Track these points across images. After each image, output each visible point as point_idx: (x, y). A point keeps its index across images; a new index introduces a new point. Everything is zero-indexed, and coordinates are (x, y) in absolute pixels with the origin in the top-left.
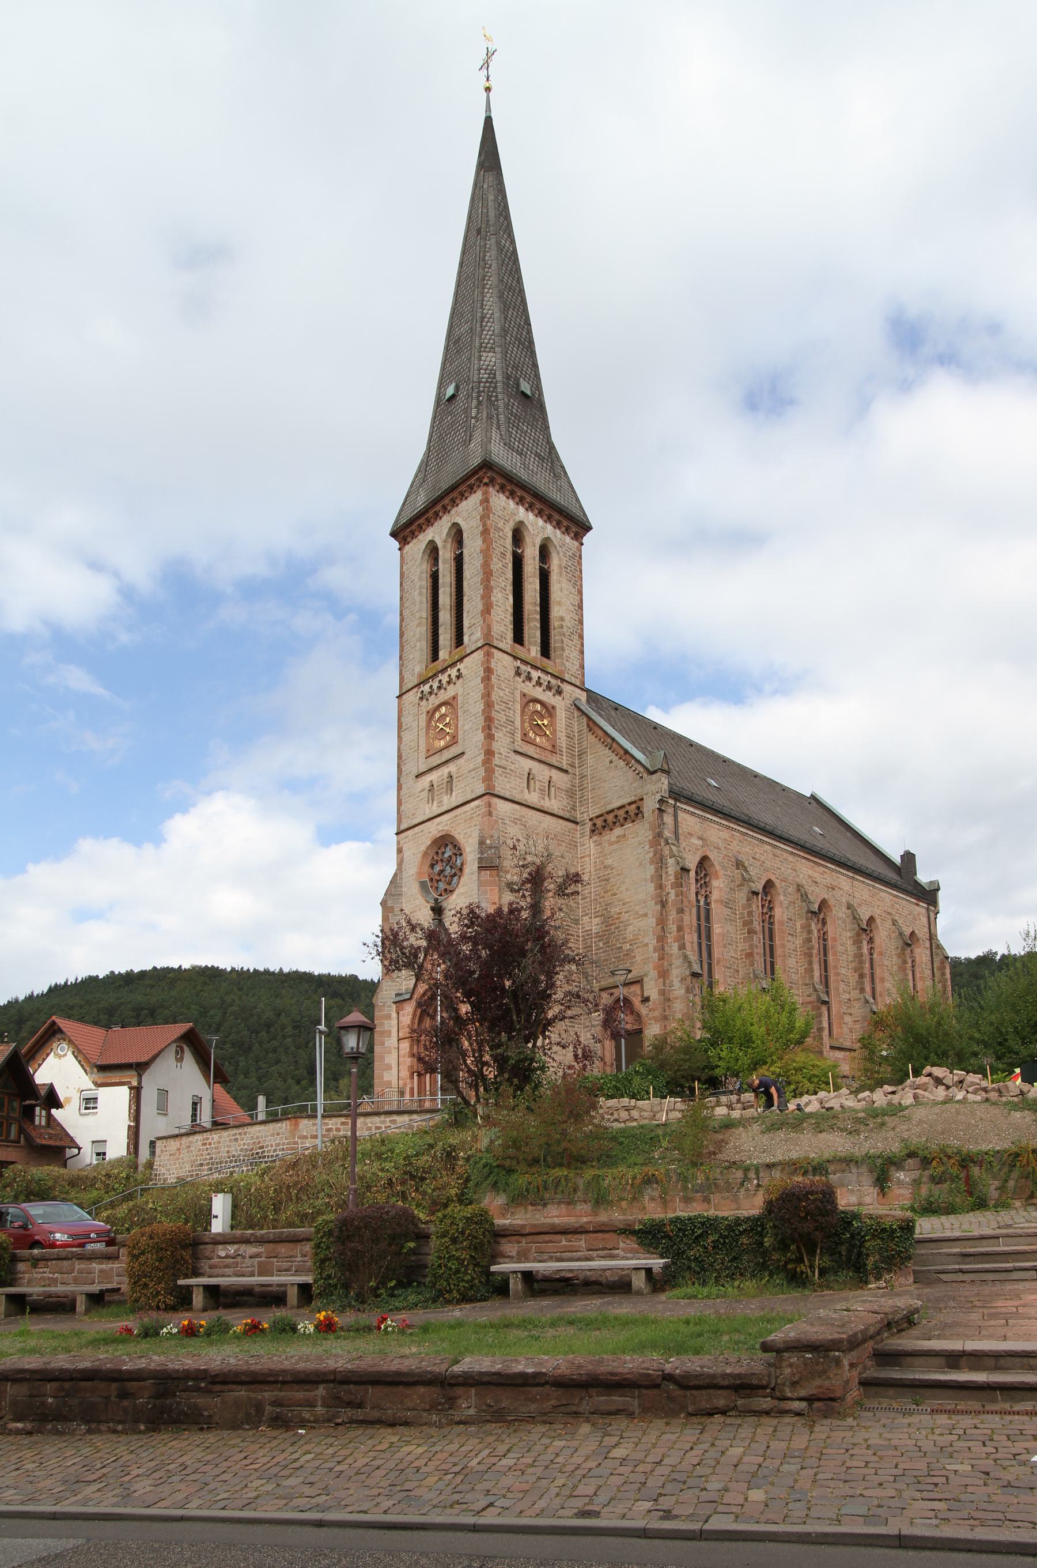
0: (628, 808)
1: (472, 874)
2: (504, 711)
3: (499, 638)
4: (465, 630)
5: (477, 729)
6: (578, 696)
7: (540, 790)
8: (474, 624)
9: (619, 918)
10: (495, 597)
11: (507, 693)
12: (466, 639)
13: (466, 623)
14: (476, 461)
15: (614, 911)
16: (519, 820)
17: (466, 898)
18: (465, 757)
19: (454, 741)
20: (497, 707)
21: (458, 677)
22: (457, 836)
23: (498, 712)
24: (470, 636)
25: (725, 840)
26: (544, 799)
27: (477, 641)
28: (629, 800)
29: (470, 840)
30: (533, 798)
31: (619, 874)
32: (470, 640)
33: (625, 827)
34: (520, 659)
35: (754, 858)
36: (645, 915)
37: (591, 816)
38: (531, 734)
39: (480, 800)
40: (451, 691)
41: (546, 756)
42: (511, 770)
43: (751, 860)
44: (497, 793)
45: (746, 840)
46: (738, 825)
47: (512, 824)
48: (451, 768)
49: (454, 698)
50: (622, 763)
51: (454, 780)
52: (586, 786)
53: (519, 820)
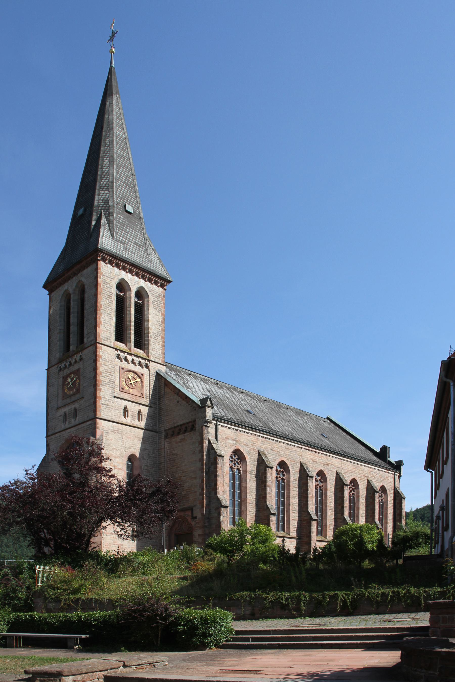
2: (108, 376)
3: (106, 339)
4: (85, 335)
5: (91, 386)
6: (159, 368)
7: (132, 416)
8: (90, 332)
10: (103, 318)
11: (110, 367)
12: (85, 340)
13: (85, 332)
16: (117, 431)
20: (103, 375)
21: (81, 359)
23: (104, 377)
24: (87, 338)
25: (252, 441)
26: (134, 420)
27: (91, 341)
30: (128, 420)
31: (181, 458)
32: (87, 341)
34: (120, 350)
35: (271, 450)
36: (195, 478)
37: (165, 429)
38: (127, 388)
39: (92, 421)
40: (76, 367)
41: (136, 399)
42: (112, 406)
43: (270, 451)
44: (103, 418)
45: (267, 441)
46: (261, 433)
47: (113, 433)
51: (78, 411)
52: (163, 414)
53: (117, 431)
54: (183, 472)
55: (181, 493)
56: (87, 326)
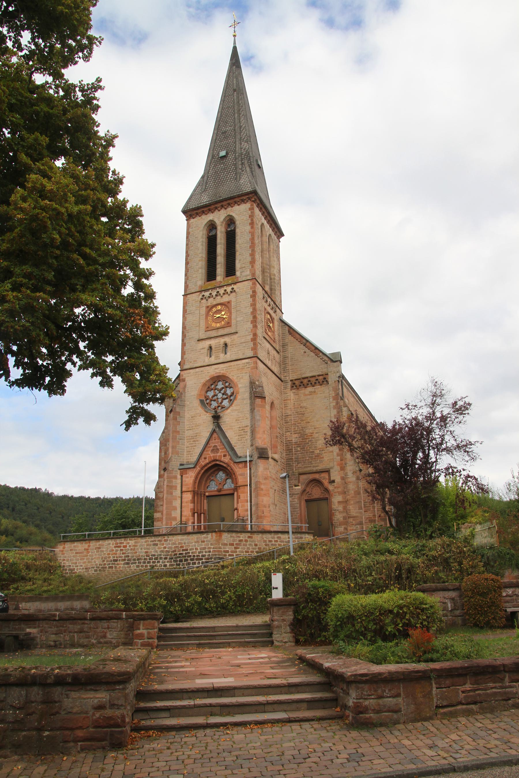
0: (317, 378)
1: (243, 399)
9: (312, 436)
14: (249, 189)
15: (308, 431)
17: (239, 412)
18: (237, 335)
19: (229, 324)
22: (231, 377)
28: (318, 374)
29: (242, 381)
33: (315, 387)
48: (227, 339)
49: (229, 302)
50: (312, 354)
54: (315, 428)
55: (314, 452)
56: (240, 260)
